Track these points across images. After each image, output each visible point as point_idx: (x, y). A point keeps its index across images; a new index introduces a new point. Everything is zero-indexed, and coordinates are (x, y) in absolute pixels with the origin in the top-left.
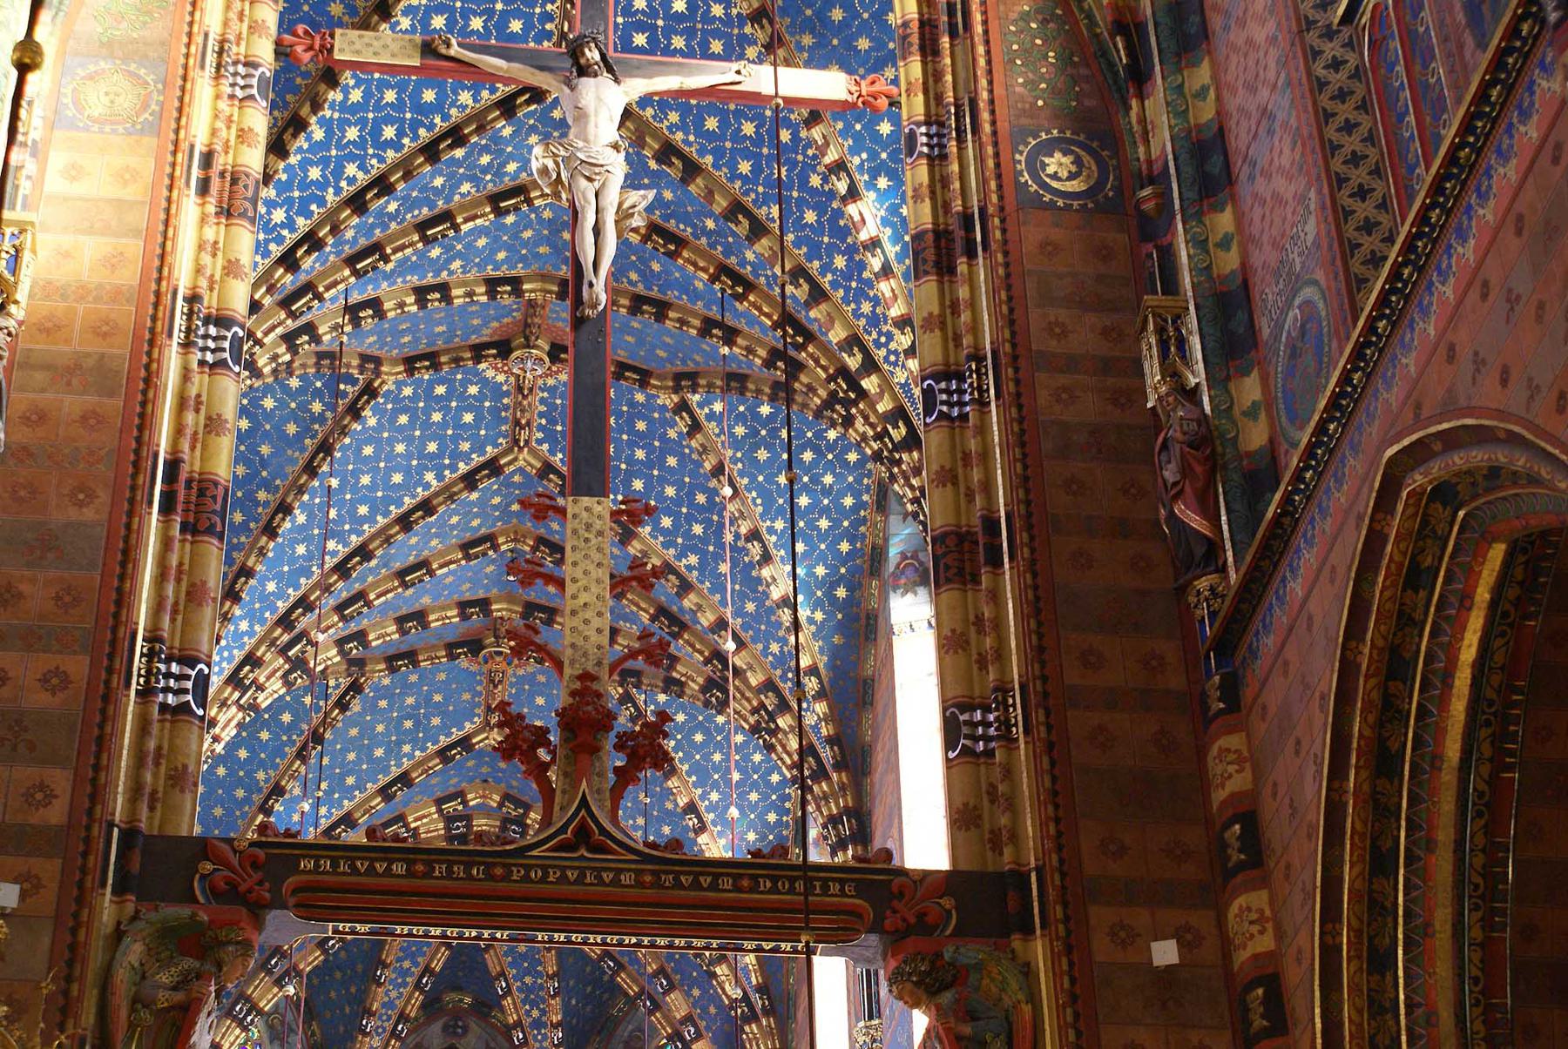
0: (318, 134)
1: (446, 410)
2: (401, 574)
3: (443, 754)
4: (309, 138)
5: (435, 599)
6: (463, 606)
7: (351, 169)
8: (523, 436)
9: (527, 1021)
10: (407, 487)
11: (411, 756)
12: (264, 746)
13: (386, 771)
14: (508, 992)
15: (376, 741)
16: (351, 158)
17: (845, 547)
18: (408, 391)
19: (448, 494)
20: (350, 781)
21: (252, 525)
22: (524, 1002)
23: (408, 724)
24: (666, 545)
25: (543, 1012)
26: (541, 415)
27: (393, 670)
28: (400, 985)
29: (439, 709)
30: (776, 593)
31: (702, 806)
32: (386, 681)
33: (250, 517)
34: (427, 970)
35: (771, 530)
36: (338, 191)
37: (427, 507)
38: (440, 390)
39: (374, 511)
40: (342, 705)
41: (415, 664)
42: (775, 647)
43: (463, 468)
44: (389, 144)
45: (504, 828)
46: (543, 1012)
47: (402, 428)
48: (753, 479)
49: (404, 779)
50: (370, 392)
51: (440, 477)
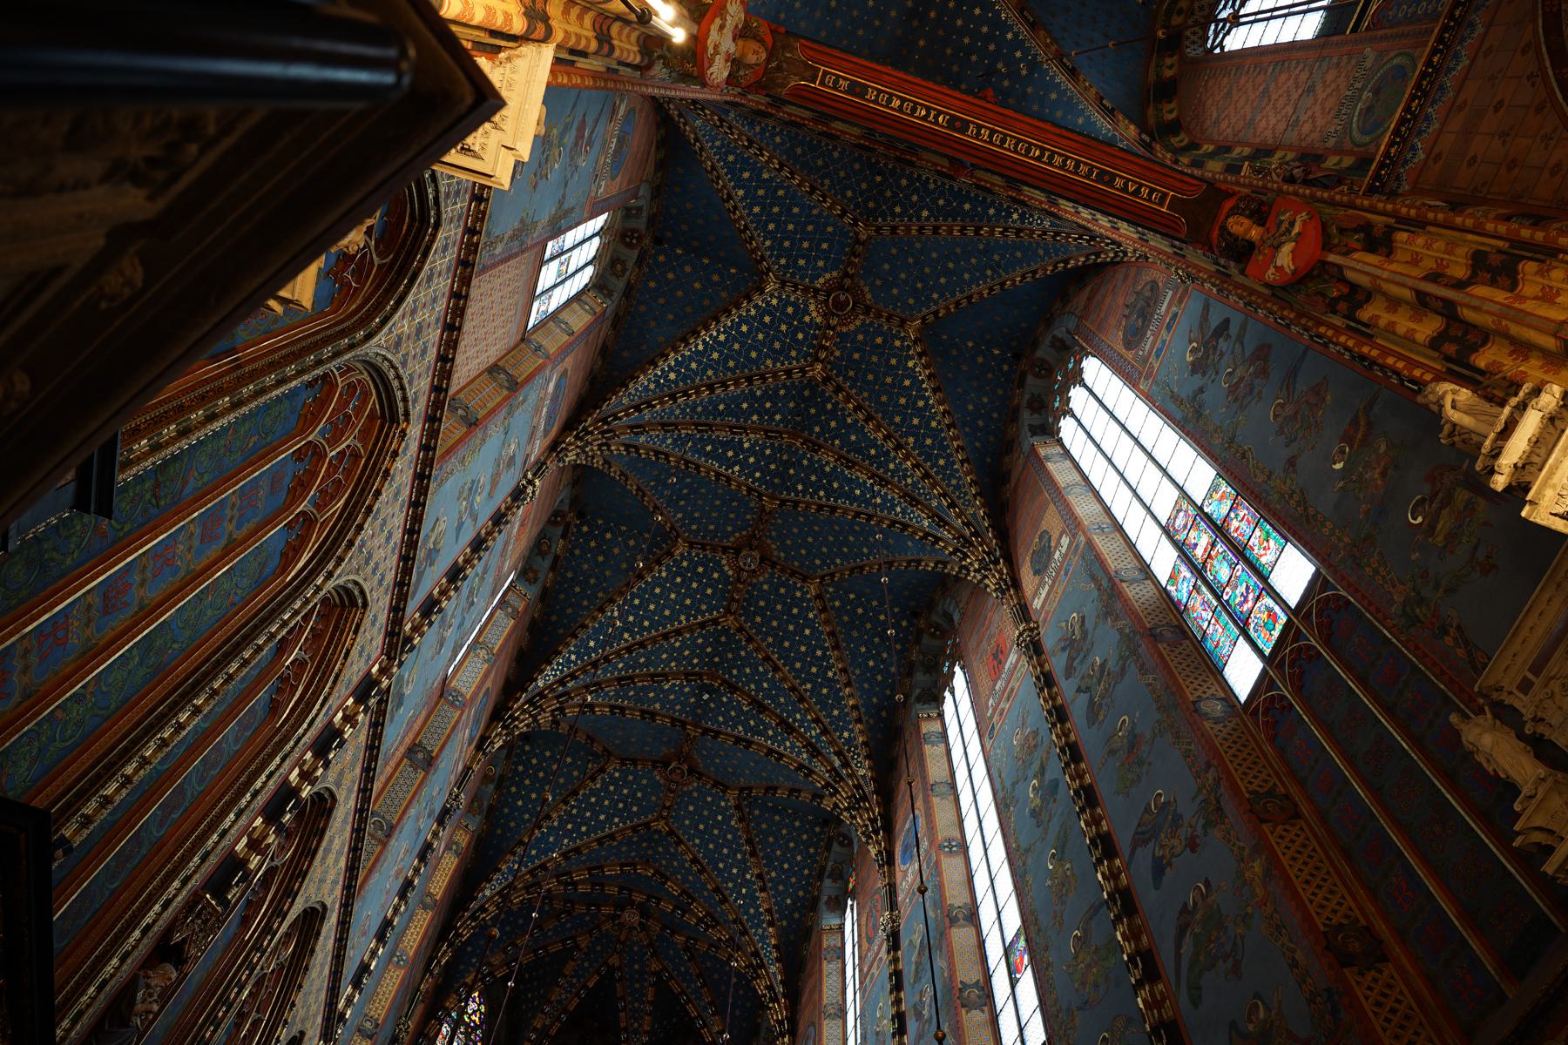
0: (701, 347)
1: (700, 582)
2: (653, 676)
3: (634, 829)
4: (696, 347)
5: (662, 707)
6: (673, 720)
7: (710, 373)
8: (734, 606)
10: (671, 619)
11: (617, 825)
14: (624, 1009)
16: (713, 368)
19: (690, 629)
23: (621, 805)
24: (795, 678)
25: (640, 1025)
26: (745, 600)
27: (623, 764)
28: (567, 992)
29: (638, 802)
34: (585, 987)
35: (853, 673)
36: (701, 380)
37: (678, 632)
38: (700, 570)
39: (651, 626)
40: (593, 779)
41: (636, 766)
42: (846, 734)
44: (729, 369)
45: (648, 900)
46: (640, 1025)
48: (848, 645)
49: (612, 837)
51: (687, 620)
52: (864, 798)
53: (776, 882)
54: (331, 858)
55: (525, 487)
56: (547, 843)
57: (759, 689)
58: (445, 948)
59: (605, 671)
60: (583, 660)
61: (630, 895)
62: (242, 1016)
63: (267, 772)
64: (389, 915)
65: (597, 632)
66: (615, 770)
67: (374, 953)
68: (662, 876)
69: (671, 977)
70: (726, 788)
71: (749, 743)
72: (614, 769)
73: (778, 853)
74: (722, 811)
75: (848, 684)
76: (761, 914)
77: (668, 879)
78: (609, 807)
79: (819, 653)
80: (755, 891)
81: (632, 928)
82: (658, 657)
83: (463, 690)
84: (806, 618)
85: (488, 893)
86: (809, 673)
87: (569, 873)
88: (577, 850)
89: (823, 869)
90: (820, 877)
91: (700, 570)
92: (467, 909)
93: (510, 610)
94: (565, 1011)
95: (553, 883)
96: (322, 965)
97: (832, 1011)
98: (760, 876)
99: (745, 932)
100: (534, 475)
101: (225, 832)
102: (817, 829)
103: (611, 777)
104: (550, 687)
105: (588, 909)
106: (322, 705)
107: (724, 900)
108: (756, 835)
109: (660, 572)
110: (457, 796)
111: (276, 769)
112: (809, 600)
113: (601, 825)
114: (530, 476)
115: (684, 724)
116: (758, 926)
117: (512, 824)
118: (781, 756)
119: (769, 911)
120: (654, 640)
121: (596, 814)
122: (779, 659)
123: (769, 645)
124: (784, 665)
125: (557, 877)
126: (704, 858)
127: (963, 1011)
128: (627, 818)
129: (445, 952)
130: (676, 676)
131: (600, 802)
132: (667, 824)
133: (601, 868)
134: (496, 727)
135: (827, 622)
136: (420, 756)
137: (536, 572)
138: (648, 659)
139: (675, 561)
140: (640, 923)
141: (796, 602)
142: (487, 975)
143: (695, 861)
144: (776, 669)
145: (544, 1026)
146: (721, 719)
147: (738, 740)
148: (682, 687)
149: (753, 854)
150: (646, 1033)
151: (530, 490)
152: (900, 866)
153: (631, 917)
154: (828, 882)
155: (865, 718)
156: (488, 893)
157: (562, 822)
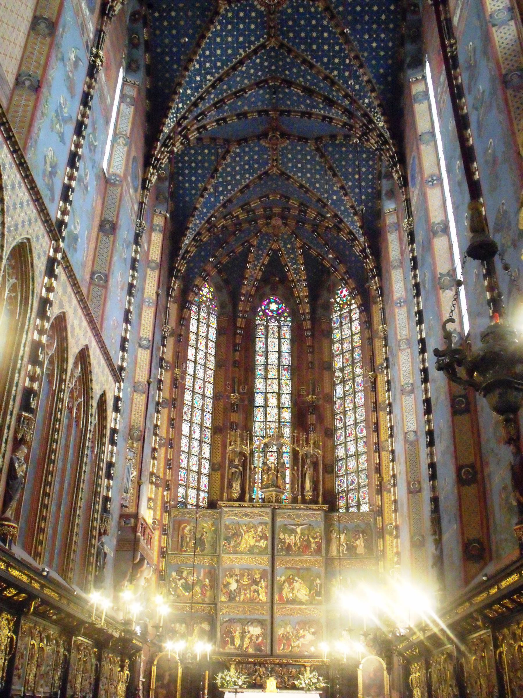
2: (235, 94)
3: (260, 178)
5: (249, 107)
6: (260, 112)
9: (295, 280)
10: (234, 54)
11: (249, 179)
12: (200, 175)
13: (241, 184)
14: (289, 270)
15: (237, 173)
17: (390, 62)
18: (230, 15)
19: (248, 57)
20: (229, 187)
21: (180, 68)
22: (294, 274)
23: (247, 167)
24: (326, 69)
25: (301, 277)
26: (278, 24)
30: (366, 78)
31: (346, 187)
32: (238, 150)
33: (179, 65)
34: (263, 264)
35: (363, 56)
37: (241, 63)
38: (242, 14)
39: (223, 65)
40: (224, 158)
43: (253, 47)
45: (283, 211)
47: (229, 31)
48: (356, 37)
49: (247, 187)
50: (217, 13)
51: (245, 51)
52: (386, 142)
53: (352, 188)
54: (77, 330)
55: (94, 62)
56: (210, 202)
57: (306, 80)
58: (173, 279)
59: (204, 105)
60: (187, 104)
61: (271, 211)
62: (70, 410)
63: (22, 345)
64: (127, 307)
65: (189, 83)
66: (236, 148)
67: (126, 330)
68: (286, 197)
69: (310, 248)
70: (306, 140)
71: (310, 115)
72: (235, 149)
73: (350, 170)
74: (310, 153)
75: (361, 66)
76: (348, 209)
77: (289, 199)
79: (337, 48)
80: (341, 196)
81: (279, 228)
82: (235, 81)
83: (118, 172)
84: (322, 26)
85: (187, 242)
86: (334, 64)
87: (230, 213)
88: (230, 201)
89: (380, 173)
90: (380, 178)
91: (242, 14)
92: (178, 255)
93: (128, 100)
94: (256, 280)
95: (223, 222)
96: (99, 363)
97: (396, 264)
98: (342, 188)
99: (341, 221)
100: (97, 48)
101: (17, 383)
103: (235, 153)
104: (173, 130)
106: (33, 296)
107: (325, 205)
108: (334, 163)
109: (215, 27)
110: (140, 224)
111: (26, 340)
112: (321, 13)
113: (239, 182)
114: (94, 50)
115: (266, 112)
116: (348, 216)
117: (187, 199)
118: (331, 119)
119: (352, 207)
120: (227, 74)
121: (233, 177)
122: (312, 59)
123: (303, 51)
124: (317, 62)
126: (306, 183)
127: (441, 291)
128: (253, 172)
129: (175, 282)
130: (250, 87)
131: (233, 168)
132: (278, 169)
133: (248, 204)
134: (149, 171)
135: (337, 26)
136: (107, 227)
137: (136, 61)
138: (228, 85)
139: (223, 16)
140: (283, 223)
141: (313, 16)
142: (206, 276)
143: (301, 186)
144: (312, 66)
145: (247, 291)
146: (289, 103)
147: (303, 114)
148: (257, 92)
149: (335, 175)
150: (304, 280)
151: (98, 62)
152: (411, 188)
153: (277, 221)
154: (384, 182)
155: (376, 87)
156: (187, 242)
157: (216, 187)
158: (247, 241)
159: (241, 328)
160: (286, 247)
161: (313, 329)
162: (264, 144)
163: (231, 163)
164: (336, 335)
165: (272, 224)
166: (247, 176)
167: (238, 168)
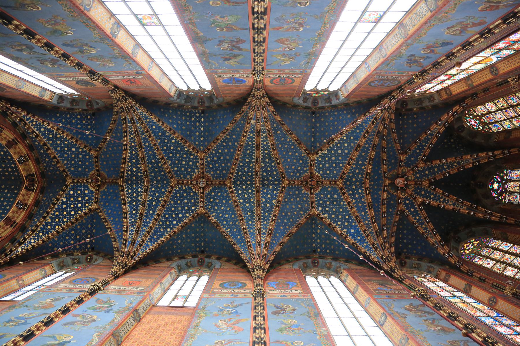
5: (275, 199)
15: (338, 211)
49: (349, 203)
77: (367, 172)
78: (336, 208)
88: (356, 217)
102: (318, 115)
103: (322, 211)
105: (401, 203)
125: (373, 223)
126: (347, 160)
128: (340, 199)
131: (334, 213)
138: (248, 211)
140: (402, 177)
158: (419, 206)
159: (501, 218)
160: (428, 175)
161: (503, 149)
162: (319, 190)
163: (328, 214)
164: (507, 125)
165: (403, 186)
166: (342, 203)
167: (334, 210)
